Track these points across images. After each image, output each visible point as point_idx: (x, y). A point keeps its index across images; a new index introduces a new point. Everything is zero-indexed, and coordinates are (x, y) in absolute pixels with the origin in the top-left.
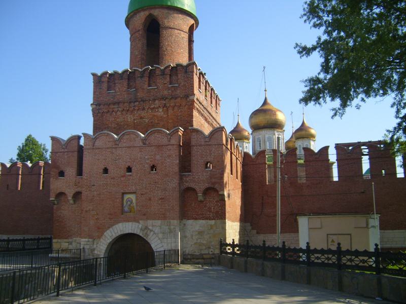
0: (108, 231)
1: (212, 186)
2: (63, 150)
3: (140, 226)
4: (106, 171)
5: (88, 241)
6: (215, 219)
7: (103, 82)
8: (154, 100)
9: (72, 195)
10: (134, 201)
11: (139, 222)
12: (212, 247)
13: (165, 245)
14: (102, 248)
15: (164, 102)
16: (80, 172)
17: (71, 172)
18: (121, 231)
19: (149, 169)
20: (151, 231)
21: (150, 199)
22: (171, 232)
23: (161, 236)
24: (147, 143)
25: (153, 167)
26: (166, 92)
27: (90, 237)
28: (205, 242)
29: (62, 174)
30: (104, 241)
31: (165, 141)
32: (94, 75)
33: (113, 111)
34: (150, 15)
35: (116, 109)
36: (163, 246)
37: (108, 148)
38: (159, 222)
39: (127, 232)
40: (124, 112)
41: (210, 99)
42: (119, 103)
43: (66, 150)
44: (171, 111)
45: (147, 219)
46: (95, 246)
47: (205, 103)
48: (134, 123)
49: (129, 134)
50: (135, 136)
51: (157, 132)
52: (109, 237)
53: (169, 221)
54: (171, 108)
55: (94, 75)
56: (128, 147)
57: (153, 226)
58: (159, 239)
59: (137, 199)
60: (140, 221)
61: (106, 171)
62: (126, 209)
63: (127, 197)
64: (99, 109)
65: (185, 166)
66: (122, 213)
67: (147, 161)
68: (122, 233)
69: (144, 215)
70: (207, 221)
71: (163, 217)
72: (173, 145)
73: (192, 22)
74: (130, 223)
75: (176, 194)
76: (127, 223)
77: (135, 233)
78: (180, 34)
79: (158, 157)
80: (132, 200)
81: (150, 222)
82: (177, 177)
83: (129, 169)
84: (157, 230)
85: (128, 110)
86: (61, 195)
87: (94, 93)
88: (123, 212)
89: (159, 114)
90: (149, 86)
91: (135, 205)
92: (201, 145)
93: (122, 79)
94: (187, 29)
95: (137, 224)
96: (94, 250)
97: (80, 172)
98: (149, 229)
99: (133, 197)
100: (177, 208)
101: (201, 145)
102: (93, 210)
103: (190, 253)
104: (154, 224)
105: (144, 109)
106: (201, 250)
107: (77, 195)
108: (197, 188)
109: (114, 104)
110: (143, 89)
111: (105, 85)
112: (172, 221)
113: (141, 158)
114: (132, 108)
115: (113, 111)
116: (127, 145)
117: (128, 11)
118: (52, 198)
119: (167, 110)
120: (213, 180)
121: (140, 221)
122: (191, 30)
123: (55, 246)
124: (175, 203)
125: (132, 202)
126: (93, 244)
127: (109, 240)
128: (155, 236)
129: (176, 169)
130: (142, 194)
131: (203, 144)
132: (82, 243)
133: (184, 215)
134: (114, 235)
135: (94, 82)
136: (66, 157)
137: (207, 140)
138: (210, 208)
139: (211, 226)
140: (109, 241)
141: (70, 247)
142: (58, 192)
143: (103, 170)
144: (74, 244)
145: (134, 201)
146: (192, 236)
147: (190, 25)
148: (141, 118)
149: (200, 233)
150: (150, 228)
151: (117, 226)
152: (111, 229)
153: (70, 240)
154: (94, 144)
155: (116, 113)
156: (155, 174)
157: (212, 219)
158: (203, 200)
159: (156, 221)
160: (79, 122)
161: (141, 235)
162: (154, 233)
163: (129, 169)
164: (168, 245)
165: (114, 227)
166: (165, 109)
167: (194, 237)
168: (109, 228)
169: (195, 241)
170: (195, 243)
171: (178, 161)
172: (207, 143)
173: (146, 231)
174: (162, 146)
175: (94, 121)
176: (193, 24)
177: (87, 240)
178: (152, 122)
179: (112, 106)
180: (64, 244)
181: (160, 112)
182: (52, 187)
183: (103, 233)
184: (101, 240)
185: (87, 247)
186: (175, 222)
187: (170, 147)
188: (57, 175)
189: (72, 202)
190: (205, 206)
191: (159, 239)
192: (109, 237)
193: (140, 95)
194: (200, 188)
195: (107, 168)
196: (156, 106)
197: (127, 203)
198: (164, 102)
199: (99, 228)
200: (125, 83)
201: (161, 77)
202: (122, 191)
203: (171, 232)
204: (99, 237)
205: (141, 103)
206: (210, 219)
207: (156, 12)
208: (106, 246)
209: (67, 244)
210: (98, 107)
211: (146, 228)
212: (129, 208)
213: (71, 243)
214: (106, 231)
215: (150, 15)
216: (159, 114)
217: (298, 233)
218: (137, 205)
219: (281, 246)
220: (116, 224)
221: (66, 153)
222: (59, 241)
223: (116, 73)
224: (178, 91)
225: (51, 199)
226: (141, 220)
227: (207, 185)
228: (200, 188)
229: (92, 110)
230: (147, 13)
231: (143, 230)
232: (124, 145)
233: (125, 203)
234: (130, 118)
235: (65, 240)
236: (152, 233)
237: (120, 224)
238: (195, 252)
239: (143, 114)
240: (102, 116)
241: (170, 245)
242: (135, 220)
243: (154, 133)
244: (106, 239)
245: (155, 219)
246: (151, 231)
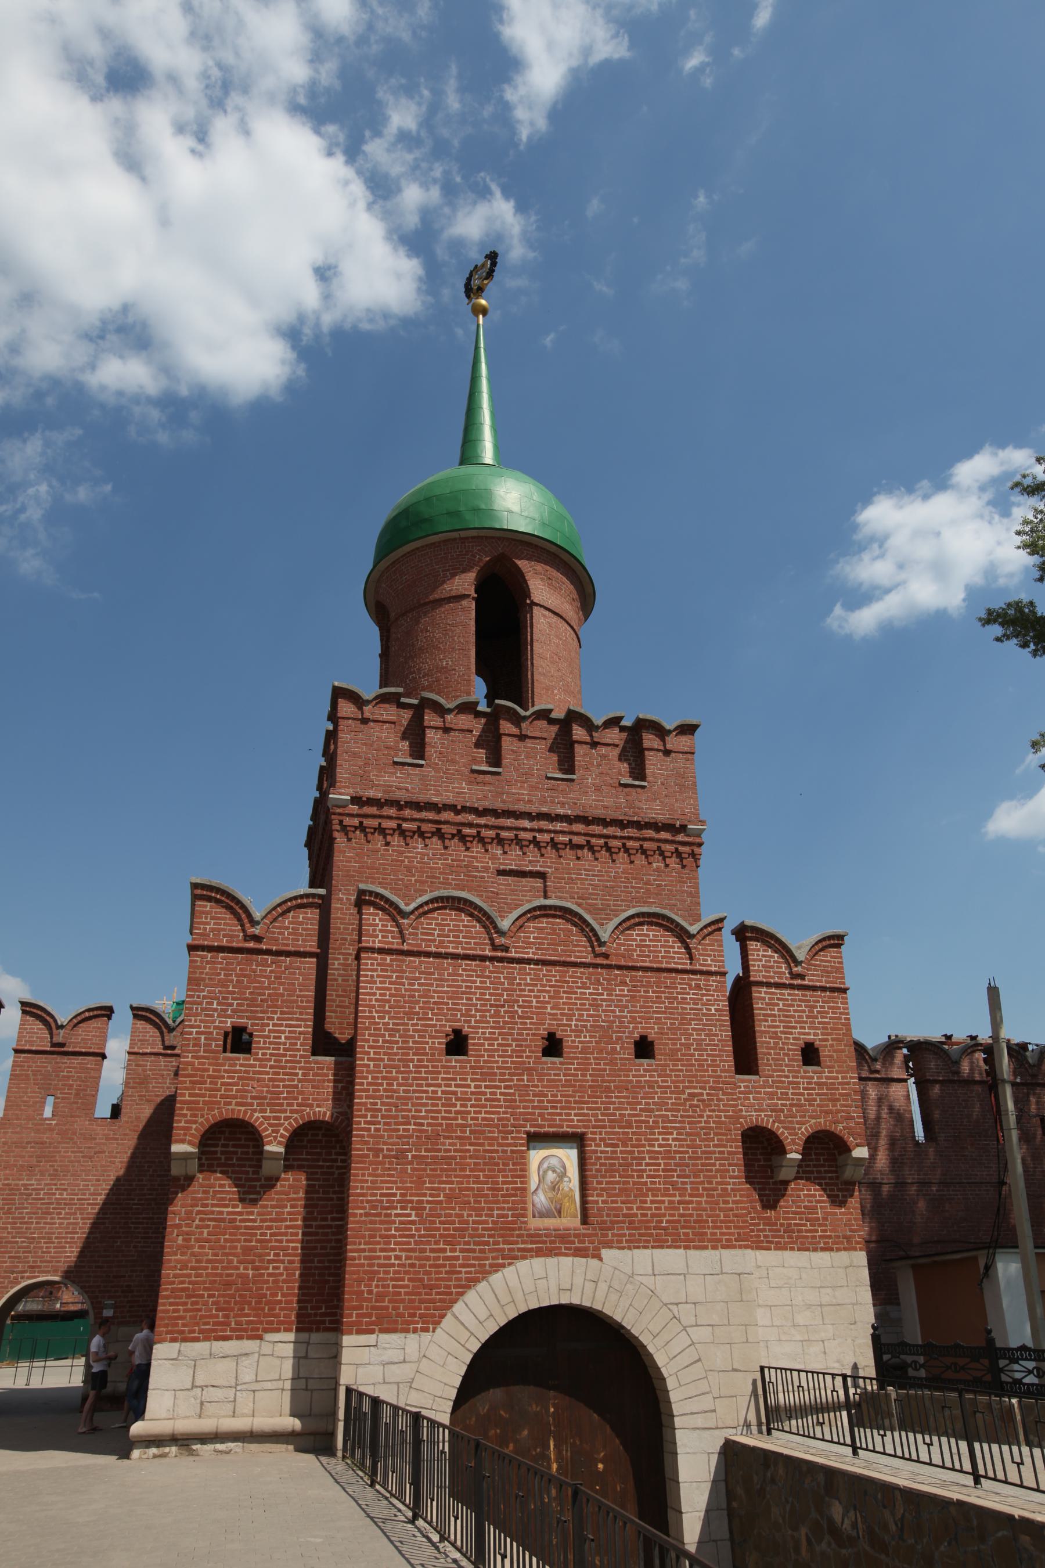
0: (471, 1296)
4: (457, 1044)
29: (239, 1041)
37: (466, 957)
51: (651, 924)
56: (545, 963)
60: (605, 1253)
61: (457, 1044)
62: (541, 1199)
68: (534, 1305)
76: (552, 1261)
80: (564, 1168)
118: (182, 1141)
121: (605, 1253)
125: (563, 1175)
132: (346, 1356)
134: (496, 1311)
157: (823, 1249)
195: (466, 1030)
196: (576, 840)
197: (541, 1180)
206: (815, 1250)
212: (551, 1200)
214: (462, 1294)
225: (176, 1148)
237: (523, 1265)
243: (641, 924)
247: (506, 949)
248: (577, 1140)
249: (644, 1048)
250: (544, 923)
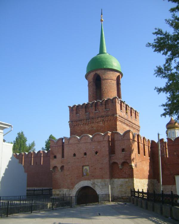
0: (76, 185)
1: (126, 161)
2: (55, 145)
3: (91, 182)
4: (75, 155)
5: (67, 190)
6: (128, 178)
7: (74, 110)
8: (98, 118)
9: (60, 167)
10: (88, 170)
11: (90, 180)
12: (127, 193)
13: (103, 192)
14: (74, 193)
15: (103, 119)
16: (63, 156)
17: (59, 156)
18: (82, 185)
19: (94, 154)
20: (96, 185)
21: (95, 169)
22: (106, 185)
23: (101, 187)
24: (93, 140)
25: (96, 153)
26: (103, 114)
27: (68, 188)
28: (124, 190)
29: (55, 157)
30: (74, 190)
31: (101, 139)
32: (69, 107)
33: (79, 125)
34: (96, 74)
36: (102, 193)
37: (75, 144)
38: (100, 180)
39: (85, 185)
40: (84, 125)
41: (130, 114)
42: (81, 120)
43: (57, 145)
44: (106, 123)
45: (95, 178)
46: (70, 193)
47: (126, 117)
48: (89, 130)
49: (84, 136)
50: (87, 137)
52: (77, 188)
53: (104, 179)
54: (106, 121)
55: (69, 107)
58: (100, 189)
59: (89, 169)
61: (75, 155)
62: (85, 174)
63: (85, 168)
64: (73, 124)
65: (112, 151)
66: (82, 176)
67: (94, 150)
68: (83, 186)
69: (93, 177)
70: (124, 179)
71: (102, 178)
72: (106, 141)
73: (118, 74)
74: (87, 181)
75: (108, 166)
76: (85, 181)
77: (89, 185)
78: (112, 82)
79: (99, 147)
81: (96, 180)
82: (108, 157)
83: (85, 154)
84: (99, 184)
85: (86, 124)
86: (55, 167)
87: (70, 116)
88: (83, 175)
89: (101, 125)
90: (95, 111)
91: (88, 171)
93: (82, 108)
94: (115, 78)
95: (90, 181)
97: (63, 156)
98: (95, 184)
99: (87, 168)
100: (108, 173)
101: (119, 140)
102: (69, 175)
103: (117, 196)
104: (98, 181)
105: (93, 123)
106: (122, 194)
107: (62, 168)
108: (118, 162)
109: (79, 121)
110: (92, 113)
111: (75, 112)
112: (106, 179)
113: (91, 148)
114: (88, 123)
115: (79, 125)
116: (84, 142)
117: (87, 71)
119: (104, 123)
120: (126, 158)
121: (91, 180)
122: (118, 79)
123: (54, 193)
124: (107, 170)
125: (87, 171)
126: (70, 192)
127: (77, 190)
128: (98, 187)
129: (108, 153)
130: (92, 166)
132: (65, 191)
133: (112, 176)
135: (69, 111)
136: (57, 149)
137: (122, 137)
138: (125, 172)
139: (127, 182)
140: (77, 190)
141: (60, 193)
142: (54, 166)
143: (74, 154)
144: (62, 192)
145: (88, 170)
146: (117, 187)
147: (117, 76)
148: (92, 127)
149: (121, 185)
150: (96, 183)
151: (80, 182)
152: (78, 184)
153: (60, 190)
154: (69, 142)
155: (80, 125)
156: (97, 156)
158: (122, 168)
159: (99, 180)
160: (62, 130)
161: (92, 187)
162: (98, 186)
163: (85, 154)
164: (104, 192)
165: (79, 183)
166: (103, 122)
167: (118, 188)
168: (77, 183)
169: (119, 190)
170: (119, 191)
171: (108, 149)
172: (122, 139)
173: (94, 185)
174: (100, 141)
175: (70, 130)
176: (119, 75)
177: (67, 189)
178: (97, 129)
179: (78, 122)
180: (58, 192)
181: (101, 124)
182: (51, 164)
183: (74, 186)
184: (73, 189)
185: (67, 193)
186: (108, 180)
187: (104, 142)
188: (53, 158)
189: (60, 171)
190: (123, 171)
191: (100, 189)
192: (77, 188)
193: (91, 115)
194: (120, 162)
197: (85, 171)
198: (103, 119)
199: (72, 184)
200: (84, 110)
201: (101, 106)
202: (82, 165)
203: (106, 185)
204: (72, 188)
205: (92, 120)
206: (126, 178)
207: (98, 72)
208: (76, 193)
209: (59, 192)
210: (72, 123)
211: (94, 183)
213: (60, 191)
215: (96, 74)
216: (101, 125)
217: (175, 184)
218: (89, 172)
219: (170, 193)
221: (57, 147)
222: (55, 190)
223: (79, 105)
224: (109, 113)
226: (92, 179)
227: (123, 161)
228: (120, 162)
229: (69, 124)
230: (94, 73)
231: (93, 185)
232: (83, 142)
233: (84, 171)
234: (87, 127)
235: (58, 190)
236: (97, 186)
237: (82, 182)
238: (119, 195)
239: (93, 125)
240: (74, 127)
241: (105, 192)
242: (89, 179)
244: (76, 189)
245: (98, 179)
246: (96, 185)
247: (80, 142)
248: (83, 166)
250: (84, 138)
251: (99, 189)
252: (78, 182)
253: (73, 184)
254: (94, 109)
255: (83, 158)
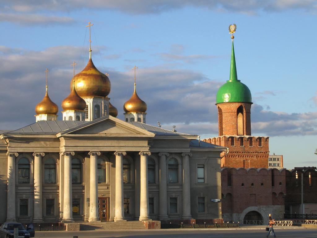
4: (243, 185)
5: (237, 215)
6: (280, 205)
11: (257, 206)
25: (262, 184)
33: (234, 156)
35: (236, 155)
38: (265, 206)
57: (262, 208)
60: (258, 206)
61: (243, 185)
67: (260, 181)
74: (254, 207)
83: (252, 184)
92: (278, 176)
95: (256, 207)
96: (239, 218)
101: (278, 176)
115: (234, 156)
121: (258, 206)
126: (239, 215)
129: (271, 185)
131: (279, 175)
152: (246, 209)
162: (263, 211)
163: (252, 184)
165: (247, 208)
168: (245, 209)
177: (236, 214)
204: (241, 213)
220: (247, 207)
249: (262, 184)
251: (264, 213)
252: (246, 208)
253: (242, 210)
254: (249, 144)
255: (250, 187)
